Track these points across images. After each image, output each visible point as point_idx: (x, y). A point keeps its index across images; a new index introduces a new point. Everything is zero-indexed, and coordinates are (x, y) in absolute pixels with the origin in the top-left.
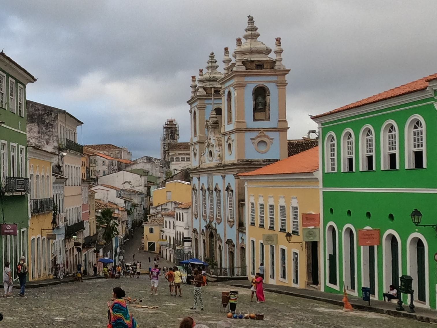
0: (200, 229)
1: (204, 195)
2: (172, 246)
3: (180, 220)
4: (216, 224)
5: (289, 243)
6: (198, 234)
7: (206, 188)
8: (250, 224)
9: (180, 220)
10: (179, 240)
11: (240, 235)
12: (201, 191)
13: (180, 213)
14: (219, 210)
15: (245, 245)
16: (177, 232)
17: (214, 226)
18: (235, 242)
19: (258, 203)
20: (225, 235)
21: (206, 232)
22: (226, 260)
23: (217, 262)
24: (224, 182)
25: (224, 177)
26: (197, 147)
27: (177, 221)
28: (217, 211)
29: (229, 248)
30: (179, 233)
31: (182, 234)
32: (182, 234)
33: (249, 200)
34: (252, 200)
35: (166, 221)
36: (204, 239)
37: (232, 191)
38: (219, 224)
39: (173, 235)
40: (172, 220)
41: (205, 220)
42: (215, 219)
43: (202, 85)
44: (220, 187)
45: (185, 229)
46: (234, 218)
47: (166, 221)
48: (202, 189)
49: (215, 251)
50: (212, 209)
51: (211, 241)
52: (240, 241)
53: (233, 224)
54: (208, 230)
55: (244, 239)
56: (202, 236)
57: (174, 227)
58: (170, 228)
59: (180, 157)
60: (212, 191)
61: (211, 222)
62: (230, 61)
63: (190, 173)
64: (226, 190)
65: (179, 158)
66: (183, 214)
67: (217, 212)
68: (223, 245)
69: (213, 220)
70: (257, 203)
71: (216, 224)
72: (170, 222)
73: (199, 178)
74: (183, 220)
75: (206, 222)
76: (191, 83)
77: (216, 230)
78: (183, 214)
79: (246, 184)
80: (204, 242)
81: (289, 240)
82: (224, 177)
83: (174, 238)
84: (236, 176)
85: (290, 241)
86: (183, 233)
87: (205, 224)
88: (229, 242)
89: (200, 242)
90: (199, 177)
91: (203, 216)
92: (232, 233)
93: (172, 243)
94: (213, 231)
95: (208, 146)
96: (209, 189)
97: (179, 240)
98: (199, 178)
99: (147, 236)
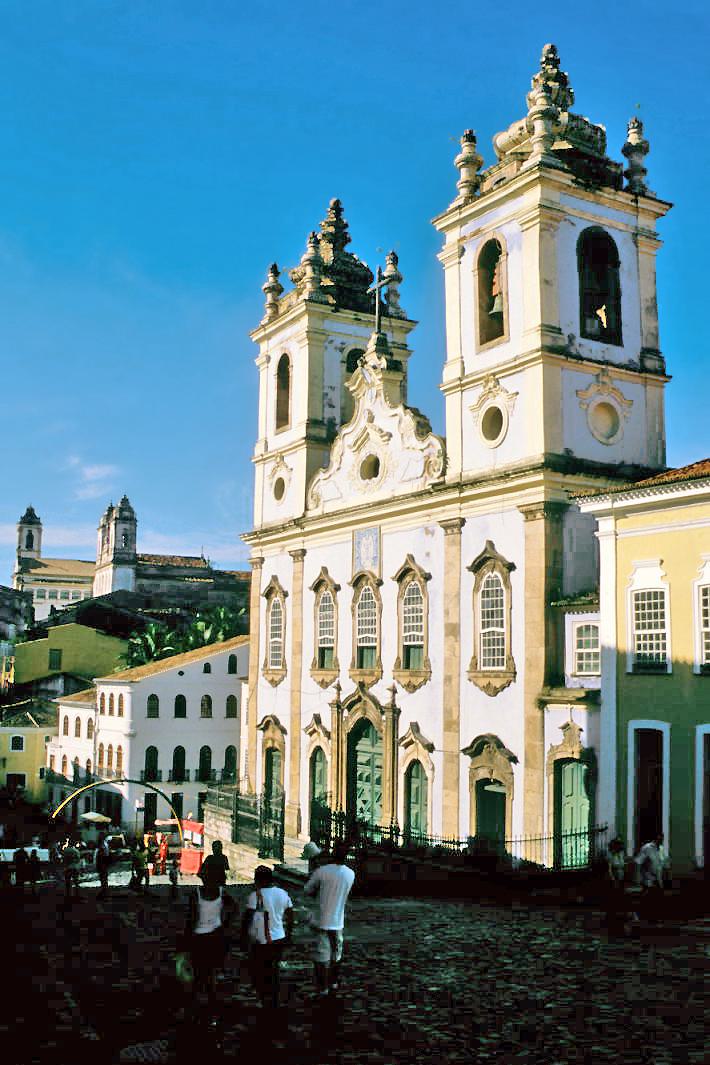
0: (296, 715)
1: (326, 607)
6: (284, 731)
7: (342, 575)
13: (112, 695)
16: (101, 745)
17: (385, 700)
18: (515, 744)
20: (451, 725)
21: (339, 721)
29: (474, 770)
31: (115, 749)
32: (115, 749)
34: (649, 579)
35: (66, 718)
36: (318, 749)
37: (511, 567)
38: (412, 688)
40: (85, 714)
41: (324, 684)
46: (511, 658)
47: (66, 718)
51: (352, 754)
56: (305, 738)
58: (78, 734)
64: (469, 569)
66: (121, 695)
71: (394, 691)
74: (121, 713)
75: (335, 691)
77: (396, 712)
78: (121, 695)
79: (606, 525)
86: (120, 748)
87: (330, 694)
89: (296, 758)
90: (304, 552)
95: (359, 445)
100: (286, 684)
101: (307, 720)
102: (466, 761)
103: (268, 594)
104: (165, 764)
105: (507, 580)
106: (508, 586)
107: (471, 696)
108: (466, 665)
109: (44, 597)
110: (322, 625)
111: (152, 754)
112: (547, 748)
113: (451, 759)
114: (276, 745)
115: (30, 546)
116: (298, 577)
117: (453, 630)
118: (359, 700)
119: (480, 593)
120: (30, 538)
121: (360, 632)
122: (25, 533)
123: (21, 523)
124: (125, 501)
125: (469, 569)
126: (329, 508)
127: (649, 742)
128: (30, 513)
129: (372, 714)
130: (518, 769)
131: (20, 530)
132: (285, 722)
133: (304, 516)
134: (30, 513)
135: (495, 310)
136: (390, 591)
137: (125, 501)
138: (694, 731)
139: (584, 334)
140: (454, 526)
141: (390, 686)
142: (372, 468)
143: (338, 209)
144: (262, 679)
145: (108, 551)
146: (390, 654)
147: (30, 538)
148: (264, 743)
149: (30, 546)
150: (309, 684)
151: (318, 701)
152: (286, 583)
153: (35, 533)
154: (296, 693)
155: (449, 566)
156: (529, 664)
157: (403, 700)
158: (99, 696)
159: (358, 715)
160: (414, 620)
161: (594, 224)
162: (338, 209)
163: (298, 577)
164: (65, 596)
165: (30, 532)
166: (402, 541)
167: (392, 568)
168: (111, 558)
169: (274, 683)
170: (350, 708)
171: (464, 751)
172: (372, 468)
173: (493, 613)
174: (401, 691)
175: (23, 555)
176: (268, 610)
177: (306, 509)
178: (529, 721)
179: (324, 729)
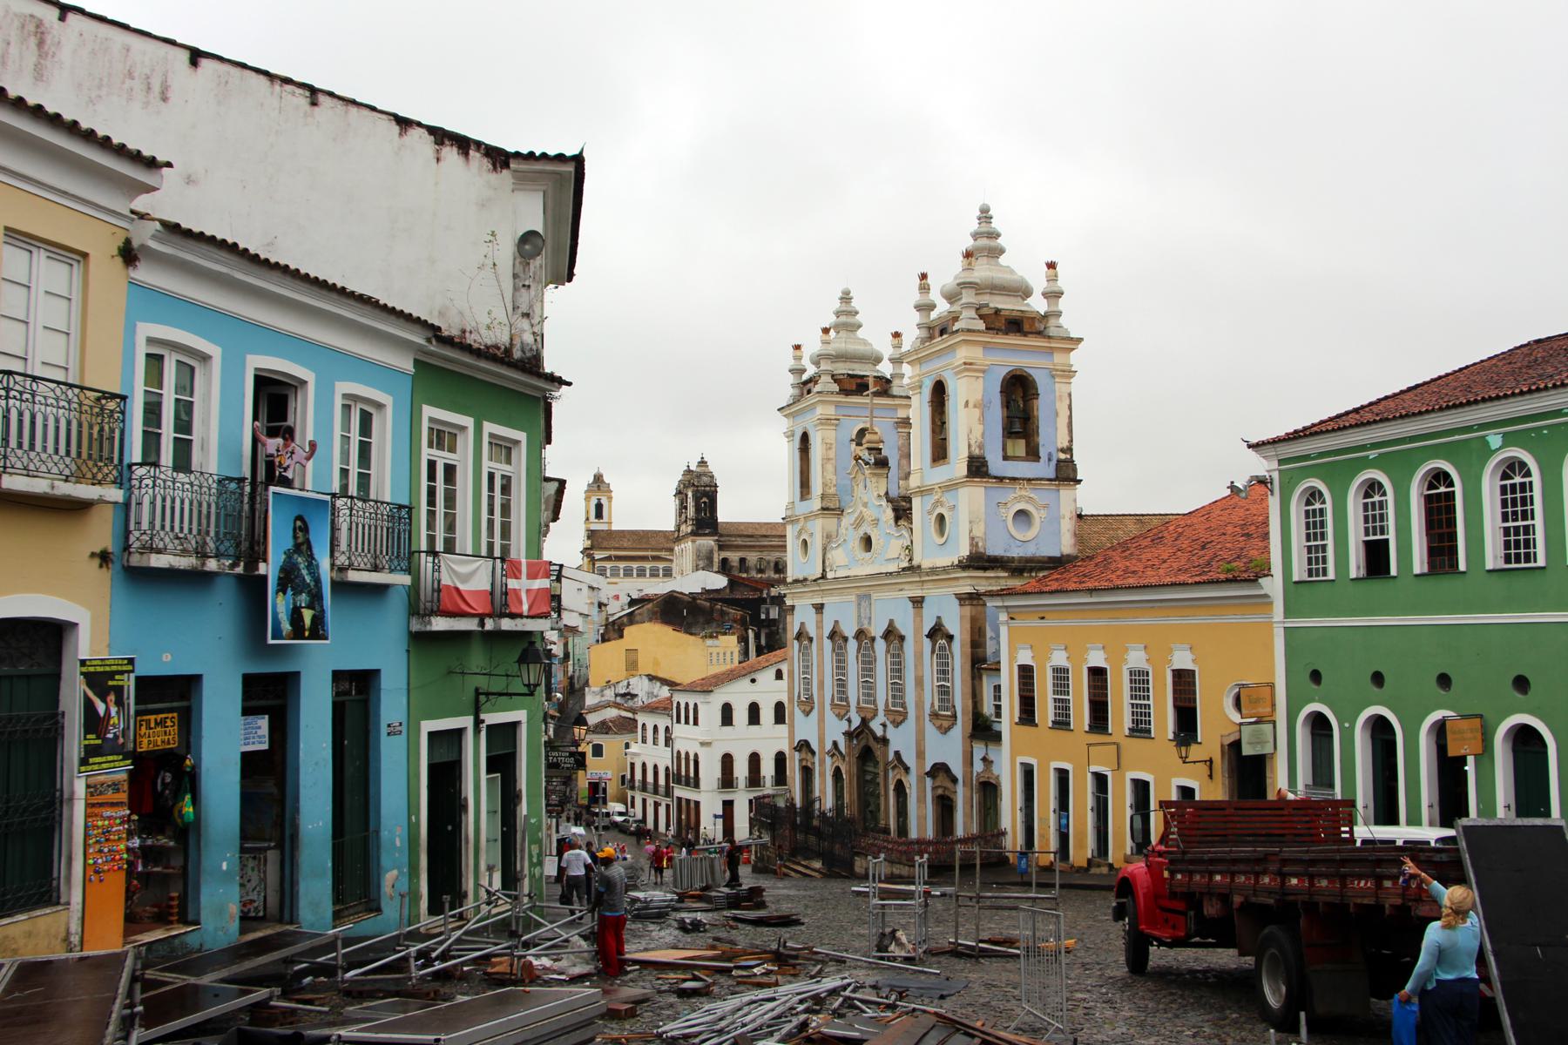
0: (821, 741)
2: (662, 790)
3: (687, 722)
4: (884, 725)
5: (1184, 762)
6: (813, 753)
7: (849, 630)
8: (1017, 720)
9: (687, 722)
10: (683, 773)
11: (979, 750)
12: (828, 644)
13: (687, 704)
14: (897, 690)
15: (998, 777)
16: (679, 752)
17: (879, 732)
18: (957, 769)
19: (1048, 665)
20: (920, 755)
21: (848, 746)
22: (922, 819)
23: (887, 824)
24: (919, 616)
25: (918, 602)
26: (818, 527)
27: (676, 725)
28: (890, 691)
29: (934, 789)
30: (683, 756)
31: (692, 757)
32: (692, 757)
33: (1012, 658)
34: (1025, 658)
35: (644, 725)
37: (950, 638)
38: (897, 724)
40: (663, 722)
42: (881, 713)
43: (829, 368)
44: (905, 626)
46: (954, 707)
47: (644, 725)
48: (833, 635)
49: (882, 799)
50: (868, 687)
51: (862, 772)
52: (978, 766)
53: (954, 724)
54: (855, 742)
55: (992, 762)
56: (828, 760)
59: (622, 565)
60: (873, 639)
61: (865, 722)
62: (932, 307)
63: (785, 595)
64: (927, 636)
65: (618, 569)
66: (696, 705)
67: (890, 693)
68: (911, 782)
69: (875, 716)
70: (1044, 668)
72: (656, 728)
73: (819, 608)
74: (696, 723)
76: (791, 363)
77: (884, 741)
80: (837, 774)
81: (1184, 755)
82: (918, 602)
83: (667, 769)
84: (964, 599)
85: (1186, 757)
86: (696, 755)
87: (844, 726)
88: (940, 769)
89: (822, 775)
91: (833, 705)
92: (949, 748)
93: (662, 781)
94: (876, 747)
96: (860, 634)
97: (683, 773)
98: (819, 608)
100: (815, 713)
101: (829, 746)
102: (929, 781)
103: (800, 636)
104: (741, 771)
105: (950, 646)
106: (952, 654)
107: (930, 729)
108: (927, 710)
109: (618, 575)
110: (838, 668)
111: (727, 761)
112: (975, 774)
113: (921, 781)
114: (809, 765)
115: (599, 515)
116: (820, 625)
117: (919, 682)
118: (862, 732)
120: (599, 507)
121: (863, 676)
122: (594, 501)
123: (586, 492)
125: (927, 636)
126: (841, 573)
127: (1028, 772)
128: (598, 479)
129: (872, 744)
130: (960, 788)
131: (587, 499)
132: (815, 746)
133: (823, 577)
134: (598, 479)
135: (942, 437)
136: (880, 645)
137: (703, 463)
138: (1049, 765)
139: (1006, 458)
140: (918, 602)
141: (882, 722)
142: (867, 542)
143: (846, 298)
144: (796, 709)
145: (686, 521)
146: (882, 695)
147: (599, 507)
148: (801, 761)
149: (599, 515)
150: (830, 716)
151: (836, 730)
152: (812, 632)
153: (604, 501)
154: (821, 720)
155: (918, 629)
156: (963, 714)
157: (891, 733)
158: (675, 705)
159: (863, 743)
160: (897, 670)
162: (846, 298)
163: (820, 625)
165: (599, 499)
166: (890, 608)
167: (878, 630)
168: (689, 529)
170: (857, 736)
171: (927, 774)
172: (867, 542)
173: (944, 672)
174: (890, 726)
175: (593, 527)
176: (800, 651)
178: (964, 752)
179: (840, 753)
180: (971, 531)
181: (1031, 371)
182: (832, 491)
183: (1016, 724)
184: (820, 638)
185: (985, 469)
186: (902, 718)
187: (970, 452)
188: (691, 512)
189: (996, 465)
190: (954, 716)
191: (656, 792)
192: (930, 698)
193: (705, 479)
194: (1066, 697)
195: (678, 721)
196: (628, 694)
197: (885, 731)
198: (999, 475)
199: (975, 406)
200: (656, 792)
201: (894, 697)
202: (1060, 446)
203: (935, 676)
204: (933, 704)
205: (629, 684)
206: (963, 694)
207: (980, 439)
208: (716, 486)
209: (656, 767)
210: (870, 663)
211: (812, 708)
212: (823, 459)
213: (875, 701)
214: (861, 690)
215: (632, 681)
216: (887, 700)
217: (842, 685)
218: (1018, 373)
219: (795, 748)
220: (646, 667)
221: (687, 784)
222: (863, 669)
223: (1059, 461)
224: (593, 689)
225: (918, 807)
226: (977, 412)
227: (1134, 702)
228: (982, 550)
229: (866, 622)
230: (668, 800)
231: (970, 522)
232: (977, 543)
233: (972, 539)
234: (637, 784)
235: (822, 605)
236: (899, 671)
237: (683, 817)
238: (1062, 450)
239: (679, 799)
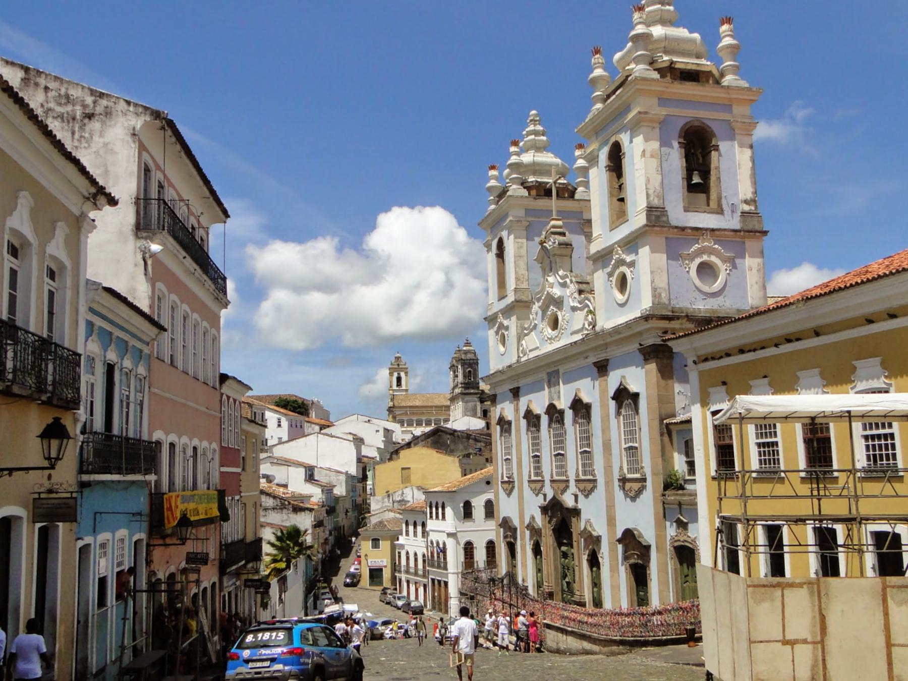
3: (437, 517)
4: (576, 496)
8: (713, 473)
9: (437, 517)
15: (694, 540)
16: (432, 542)
20: (611, 521)
39: (421, 551)
42: (572, 484)
45: (449, 535)
48: (525, 417)
53: (644, 487)
57: (425, 534)
64: (613, 398)
71: (576, 496)
75: (541, 497)
77: (576, 512)
83: (424, 556)
86: (444, 544)
87: (540, 501)
95: (544, 309)
99: (366, 555)
100: (515, 492)
108: (616, 476)
111: (469, 549)
117: (607, 447)
119: (622, 417)
120: (399, 379)
121: (556, 449)
122: (396, 375)
124: (468, 344)
132: (516, 522)
142: (555, 324)
152: (509, 415)
153: (403, 375)
156: (654, 474)
161: (692, 119)
164: (428, 423)
165: (399, 374)
169: (509, 493)
172: (555, 324)
173: (631, 433)
174: (581, 497)
177: (519, 357)
180: (653, 282)
181: (709, 123)
182: (525, 285)
183: (714, 478)
184: (517, 420)
185: (664, 219)
186: (591, 485)
187: (648, 202)
188: (460, 378)
189: (678, 215)
190: (644, 480)
191: (416, 574)
192: (620, 462)
193: (470, 356)
194: (773, 440)
195: (431, 517)
196: (403, 500)
197: (576, 500)
198: (680, 225)
199: (652, 156)
200: (416, 574)
201: (584, 465)
202: (742, 196)
203: (623, 437)
204: (621, 468)
205: (403, 493)
206: (652, 453)
207: (658, 188)
208: (477, 359)
209: (416, 554)
210: (561, 435)
211: (513, 487)
212: (515, 256)
213: (566, 472)
214: (554, 464)
215: (405, 491)
216: (577, 469)
217: (537, 458)
218: (696, 124)
219: (500, 525)
220: (415, 477)
221: (439, 567)
222: (555, 443)
223: (743, 213)
224: (376, 497)
225: (612, 577)
226: (654, 163)
227: (869, 432)
228: (666, 301)
229: (555, 396)
230: (425, 580)
231: (652, 272)
232: (660, 295)
233: (654, 290)
234: (403, 569)
235: (518, 388)
236: (588, 438)
237: (436, 594)
238: (746, 202)
239: (433, 580)
